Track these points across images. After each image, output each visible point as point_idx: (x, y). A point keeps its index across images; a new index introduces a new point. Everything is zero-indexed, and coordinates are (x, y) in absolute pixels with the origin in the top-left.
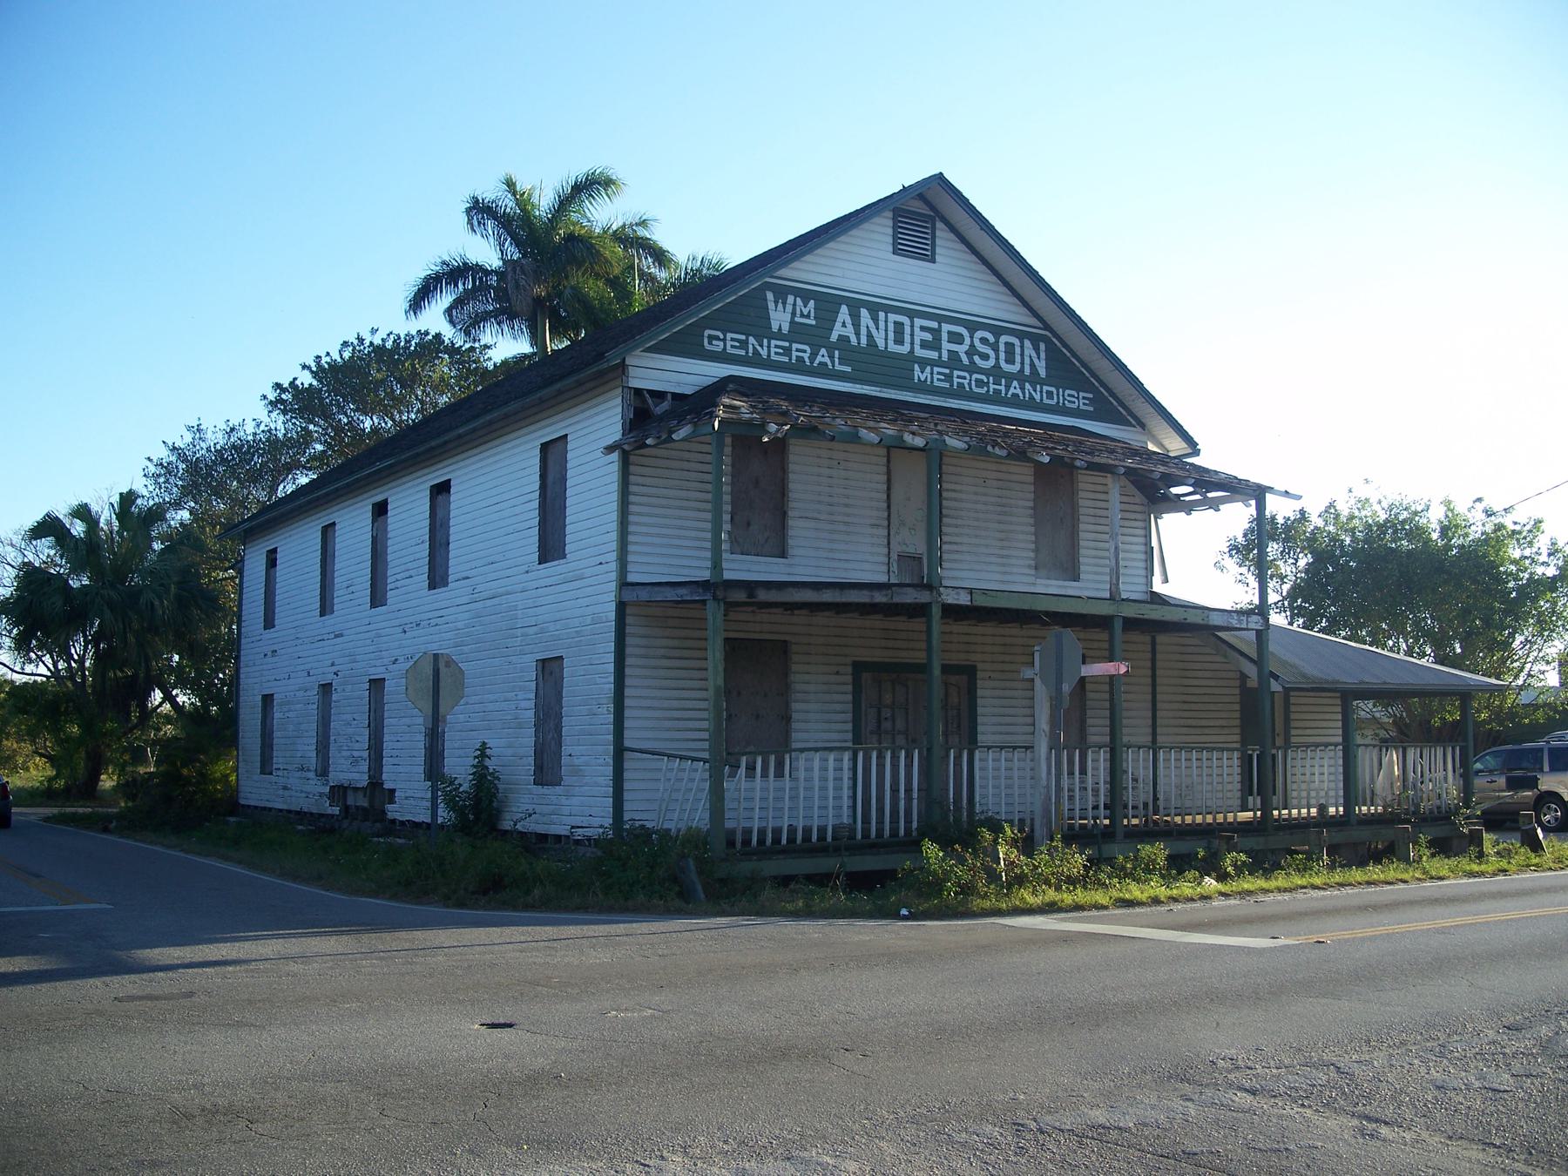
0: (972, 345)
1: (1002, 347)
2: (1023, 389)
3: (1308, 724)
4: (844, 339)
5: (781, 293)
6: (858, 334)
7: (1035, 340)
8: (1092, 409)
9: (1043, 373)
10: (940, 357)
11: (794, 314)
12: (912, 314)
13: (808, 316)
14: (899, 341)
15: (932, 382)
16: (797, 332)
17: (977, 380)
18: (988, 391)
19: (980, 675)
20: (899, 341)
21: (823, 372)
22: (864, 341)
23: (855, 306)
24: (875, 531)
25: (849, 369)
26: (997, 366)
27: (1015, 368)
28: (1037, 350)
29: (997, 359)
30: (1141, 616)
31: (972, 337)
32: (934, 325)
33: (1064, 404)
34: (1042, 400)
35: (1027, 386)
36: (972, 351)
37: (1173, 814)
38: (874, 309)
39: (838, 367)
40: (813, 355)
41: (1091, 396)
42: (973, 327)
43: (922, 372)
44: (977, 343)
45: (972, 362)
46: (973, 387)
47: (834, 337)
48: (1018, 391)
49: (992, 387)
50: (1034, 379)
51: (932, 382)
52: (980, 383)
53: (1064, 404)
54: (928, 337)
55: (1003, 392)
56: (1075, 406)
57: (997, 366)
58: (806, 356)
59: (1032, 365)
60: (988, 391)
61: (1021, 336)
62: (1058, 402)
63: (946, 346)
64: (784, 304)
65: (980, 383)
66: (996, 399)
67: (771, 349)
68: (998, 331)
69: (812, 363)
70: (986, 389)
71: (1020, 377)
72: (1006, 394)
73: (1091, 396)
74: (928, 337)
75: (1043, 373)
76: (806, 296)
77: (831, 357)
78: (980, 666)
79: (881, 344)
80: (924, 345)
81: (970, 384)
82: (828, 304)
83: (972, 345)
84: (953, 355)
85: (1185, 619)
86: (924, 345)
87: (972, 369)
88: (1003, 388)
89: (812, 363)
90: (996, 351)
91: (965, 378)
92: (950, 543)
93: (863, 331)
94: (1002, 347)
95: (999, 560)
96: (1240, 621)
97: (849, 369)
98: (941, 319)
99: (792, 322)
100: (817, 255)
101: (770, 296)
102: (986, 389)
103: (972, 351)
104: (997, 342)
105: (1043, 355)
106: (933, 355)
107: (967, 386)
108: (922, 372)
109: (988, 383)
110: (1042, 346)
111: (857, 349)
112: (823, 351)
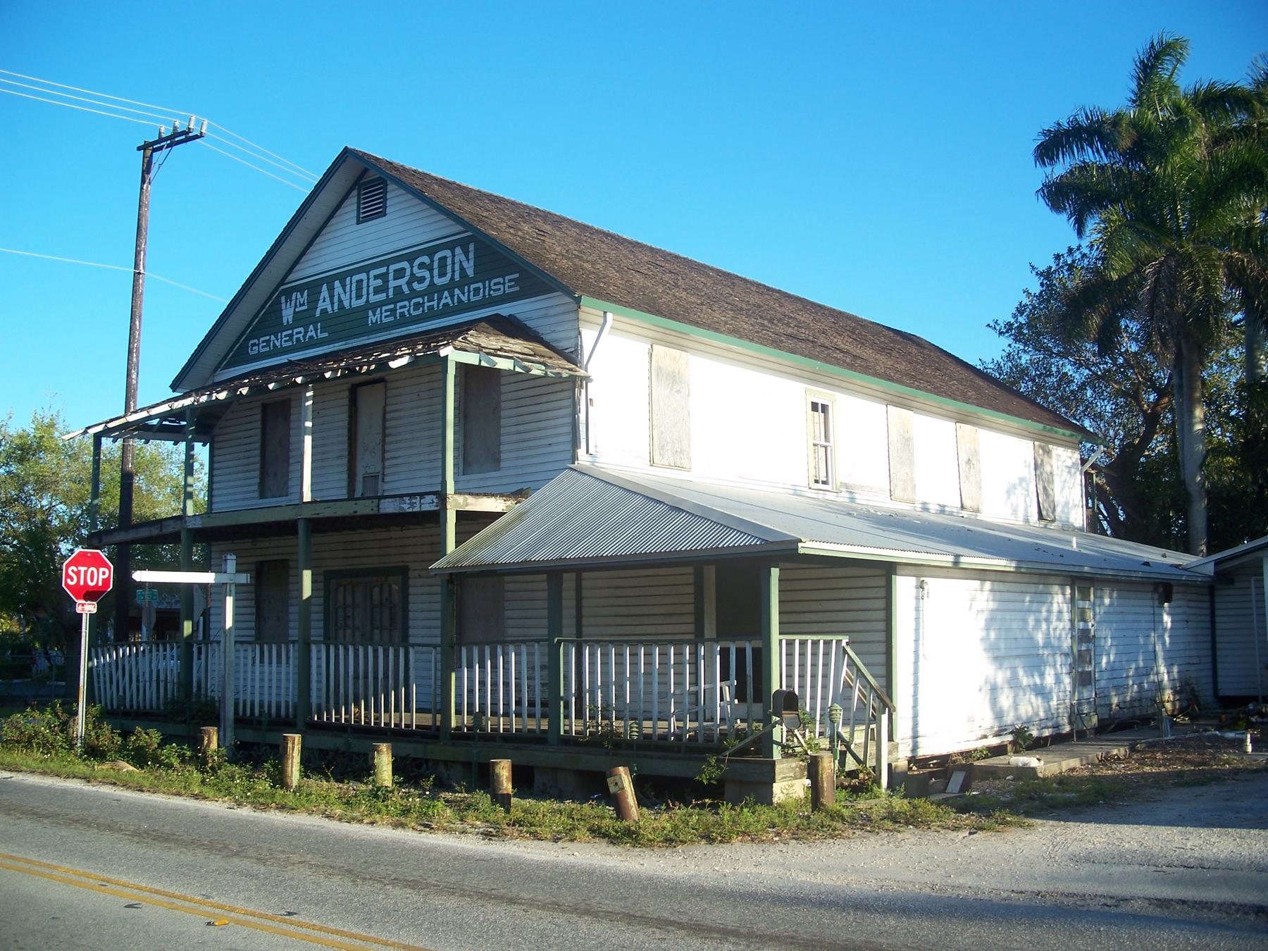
0: (412, 274)
1: (436, 265)
2: (452, 296)
3: (806, 606)
4: (324, 311)
5: (288, 293)
6: (332, 304)
7: (463, 244)
8: (517, 289)
9: (470, 273)
10: (387, 296)
11: (296, 306)
12: (367, 269)
13: (303, 304)
14: (359, 297)
15: (381, 321)
16: (302, 319)
17: (415, 304)
18: (423, 311)
19: (411, 574)
20: (359, 297)
21: (314, 343)
22: (336, 307)
23: (330, 281)
24: (339, 462)
25: (326, 335)
26: (432, 284)
27: (446, 280)
28: (466, 253)
29: (432, 277)
30: (317, 516)
31: (412, 267)
32: (383, 270)
33: (490, 295)
34: (469, 300)
35: (457, 291)
36: (413, 278)
37: (655, 715)
38: (342, 277)
39: (320, 336)
40: (306, 332)
41: (517, 276)
42: (410, 258)
43: (374, 315)
44: (416, 270)
45: (411, 289)
46: (412, 312)
47: (318, 313)
48: (449, 300)
49: (427, 304)
50: (465, 281)
51: (381, 321)
52: (417, 306)
53: (490, 295)
54: (379, 282)
55: (450, 302)
56: (500, 293)
57: (432, 284)
58: (300, 336)
59: (462, 269)
60: (423, 311)
61: (451, 246)
62: (484, 296)
63: (392, 284)
64: (291, 301)
65: (417, 306)
66: (432, 315)
67: (281, 341)
68: (430, 252)
69: (305, 339)
70: (421, 309)
71: (450, 287)
72: (438, 307)
73: (517, 276)
74: (379, 282)
75: (470, 273)
76: (300, 289)
77: (316, 330)
78: (412, 566)
79: (346, 304)
80: (377, 291)
81: (409, 311)
82: (313, 288)
83: (412, 274)
84: (398, 289)
85: (356, 512)
86: (377, 291)
87: (414, 294)
88: (435, 303)
89: (305, 339)
90: (431, 270)
91: (405, 307)
92: (392, 458)
93: (336, 299)
94: (436, 265)
95: (429, 465)
96: (412, 505)
97: (326, 335)
98: (386, 263)
99: (295, 313)
100: (311, 252)
101: (283, 299)
102: (421, 309)
103: (413, 278)
104: (432, 261)
105: (471, 255)
106: (382, 296)
107: (406, 313)
108: (374, 315)
109: (424, 303)
110: (471, 247)
111: (335, 316)
112: (311, 327)
